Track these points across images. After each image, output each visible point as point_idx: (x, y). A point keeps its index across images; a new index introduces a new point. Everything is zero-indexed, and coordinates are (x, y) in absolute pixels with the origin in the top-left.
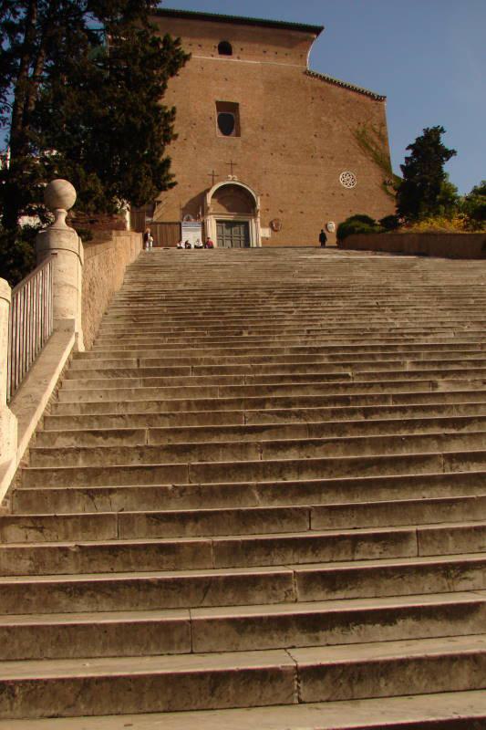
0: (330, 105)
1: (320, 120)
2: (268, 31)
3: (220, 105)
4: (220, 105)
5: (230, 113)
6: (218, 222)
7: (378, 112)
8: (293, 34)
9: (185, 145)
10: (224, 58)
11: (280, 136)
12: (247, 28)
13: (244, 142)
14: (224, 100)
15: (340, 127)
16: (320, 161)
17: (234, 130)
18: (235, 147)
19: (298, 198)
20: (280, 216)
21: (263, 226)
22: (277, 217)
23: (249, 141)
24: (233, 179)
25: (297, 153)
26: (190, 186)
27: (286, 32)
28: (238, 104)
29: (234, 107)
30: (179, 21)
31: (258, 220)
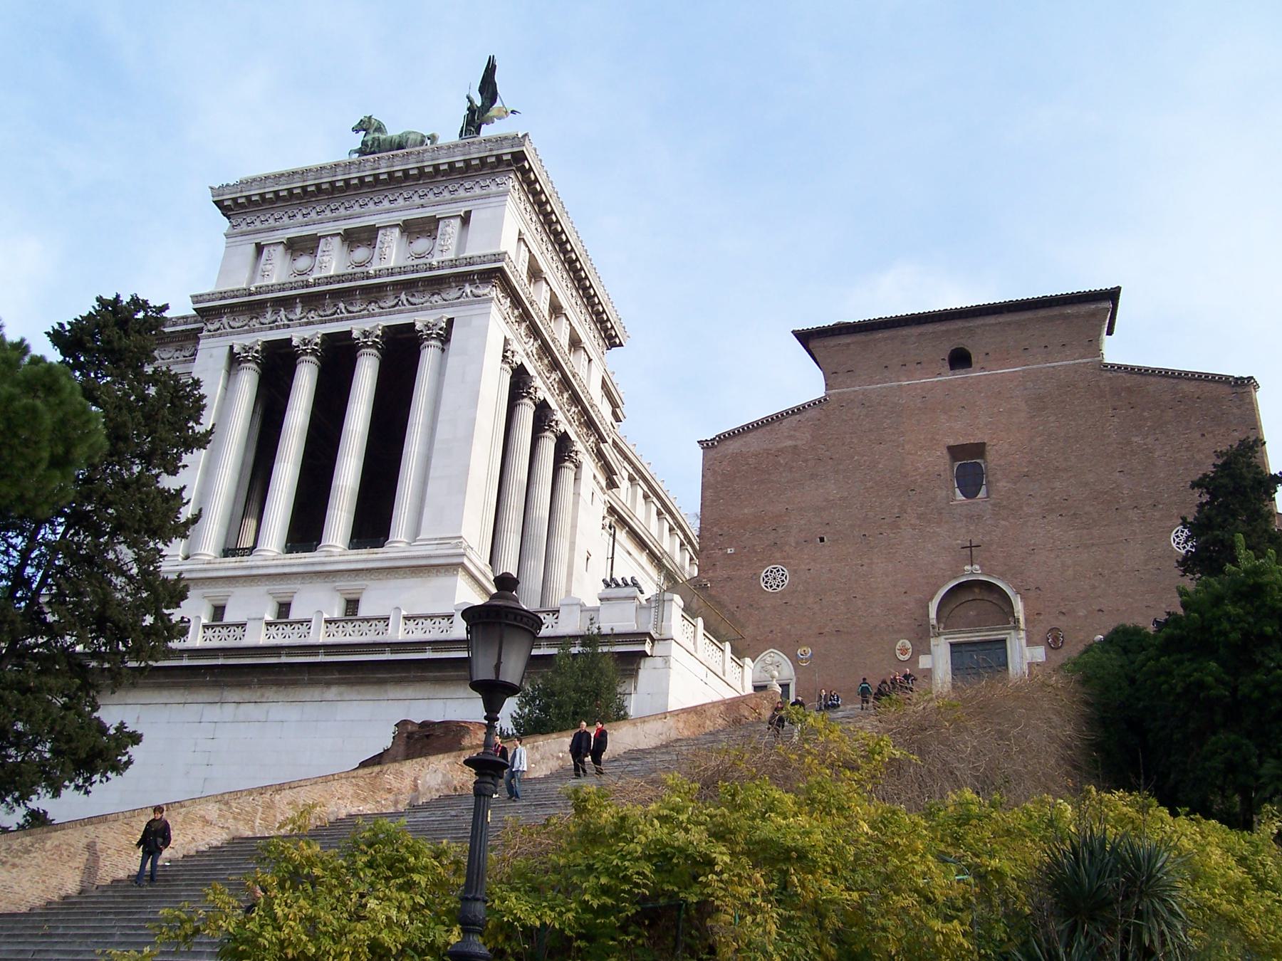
0: (1146, 414)
1: (1129, 443)
2: (1028, 315)
3: (956, 452)
4: (956, 452)
5: (978, 461)
6: (951, 644)
7: (1239, 407)
8: (1069, 310)
9: (898, 527)
10: (960, 375)
11: (1057, 484)
12: (991, 320)
13: (992, 505)
14: (962, 441)
15: (1168, 448)
16: (1133, 515)
17: (984, 488)
18: (980, 517)
19: (1094, 587)
20: (1062, 623)
21: (1031, 642)
22: (1056, 624)
23: (1005, 503)
24: (973, 572)
25: (1087, 509)
26: (905, 593)
27: (1055, 311)
28: (984, 444)
29: (978, 450)
30: (880, 335)
31: (1023, 634)
